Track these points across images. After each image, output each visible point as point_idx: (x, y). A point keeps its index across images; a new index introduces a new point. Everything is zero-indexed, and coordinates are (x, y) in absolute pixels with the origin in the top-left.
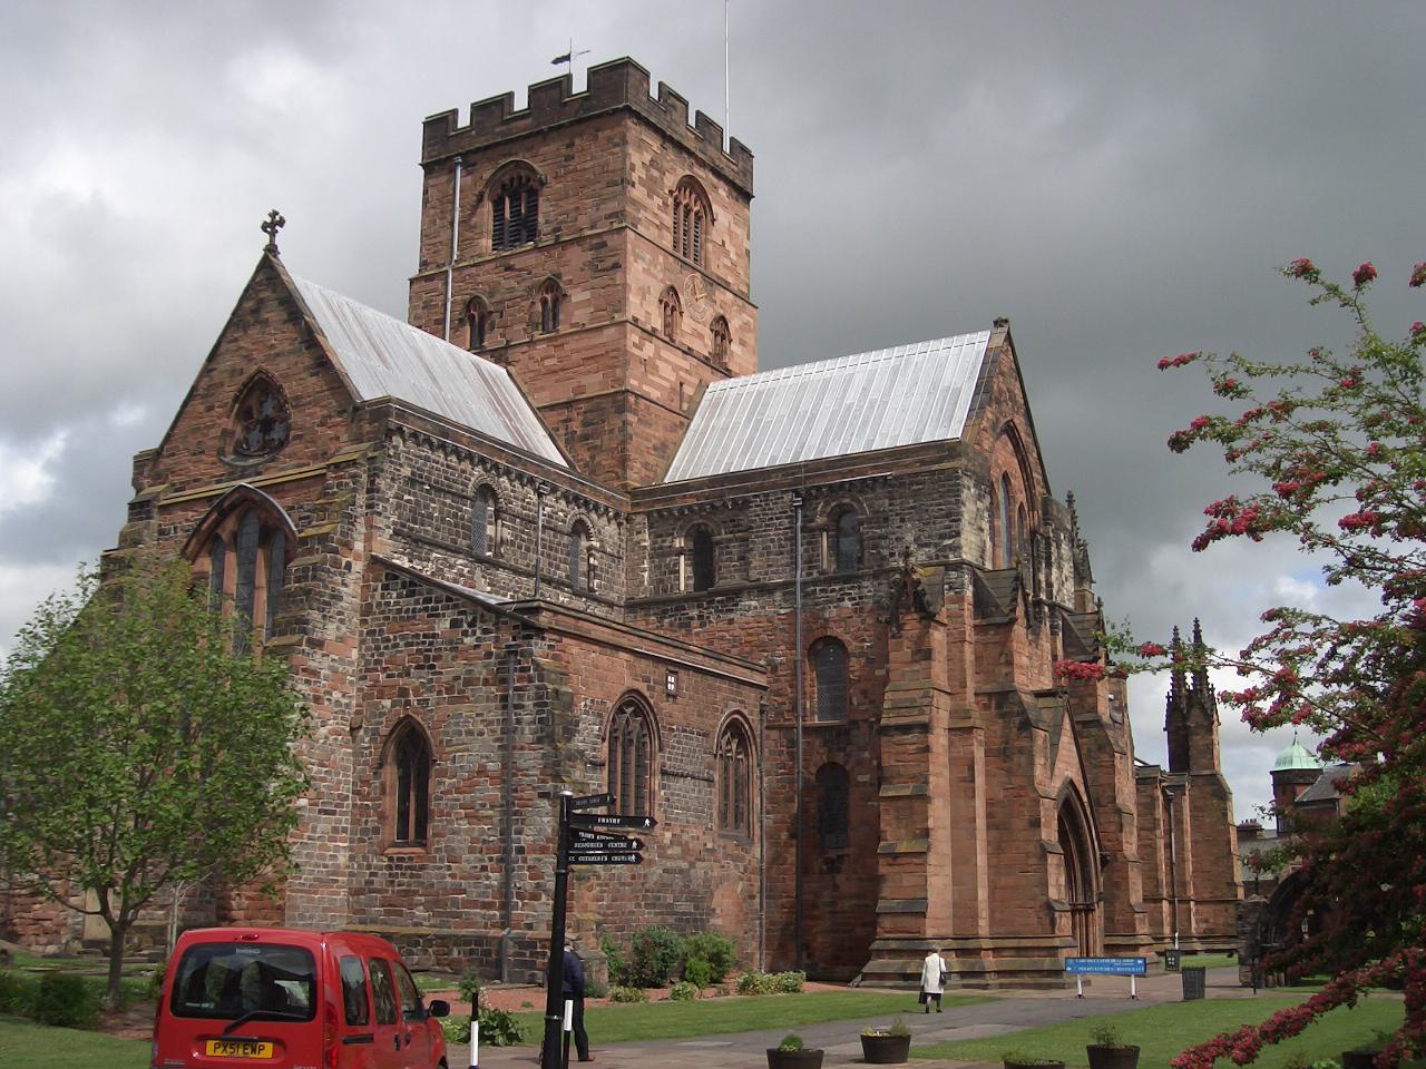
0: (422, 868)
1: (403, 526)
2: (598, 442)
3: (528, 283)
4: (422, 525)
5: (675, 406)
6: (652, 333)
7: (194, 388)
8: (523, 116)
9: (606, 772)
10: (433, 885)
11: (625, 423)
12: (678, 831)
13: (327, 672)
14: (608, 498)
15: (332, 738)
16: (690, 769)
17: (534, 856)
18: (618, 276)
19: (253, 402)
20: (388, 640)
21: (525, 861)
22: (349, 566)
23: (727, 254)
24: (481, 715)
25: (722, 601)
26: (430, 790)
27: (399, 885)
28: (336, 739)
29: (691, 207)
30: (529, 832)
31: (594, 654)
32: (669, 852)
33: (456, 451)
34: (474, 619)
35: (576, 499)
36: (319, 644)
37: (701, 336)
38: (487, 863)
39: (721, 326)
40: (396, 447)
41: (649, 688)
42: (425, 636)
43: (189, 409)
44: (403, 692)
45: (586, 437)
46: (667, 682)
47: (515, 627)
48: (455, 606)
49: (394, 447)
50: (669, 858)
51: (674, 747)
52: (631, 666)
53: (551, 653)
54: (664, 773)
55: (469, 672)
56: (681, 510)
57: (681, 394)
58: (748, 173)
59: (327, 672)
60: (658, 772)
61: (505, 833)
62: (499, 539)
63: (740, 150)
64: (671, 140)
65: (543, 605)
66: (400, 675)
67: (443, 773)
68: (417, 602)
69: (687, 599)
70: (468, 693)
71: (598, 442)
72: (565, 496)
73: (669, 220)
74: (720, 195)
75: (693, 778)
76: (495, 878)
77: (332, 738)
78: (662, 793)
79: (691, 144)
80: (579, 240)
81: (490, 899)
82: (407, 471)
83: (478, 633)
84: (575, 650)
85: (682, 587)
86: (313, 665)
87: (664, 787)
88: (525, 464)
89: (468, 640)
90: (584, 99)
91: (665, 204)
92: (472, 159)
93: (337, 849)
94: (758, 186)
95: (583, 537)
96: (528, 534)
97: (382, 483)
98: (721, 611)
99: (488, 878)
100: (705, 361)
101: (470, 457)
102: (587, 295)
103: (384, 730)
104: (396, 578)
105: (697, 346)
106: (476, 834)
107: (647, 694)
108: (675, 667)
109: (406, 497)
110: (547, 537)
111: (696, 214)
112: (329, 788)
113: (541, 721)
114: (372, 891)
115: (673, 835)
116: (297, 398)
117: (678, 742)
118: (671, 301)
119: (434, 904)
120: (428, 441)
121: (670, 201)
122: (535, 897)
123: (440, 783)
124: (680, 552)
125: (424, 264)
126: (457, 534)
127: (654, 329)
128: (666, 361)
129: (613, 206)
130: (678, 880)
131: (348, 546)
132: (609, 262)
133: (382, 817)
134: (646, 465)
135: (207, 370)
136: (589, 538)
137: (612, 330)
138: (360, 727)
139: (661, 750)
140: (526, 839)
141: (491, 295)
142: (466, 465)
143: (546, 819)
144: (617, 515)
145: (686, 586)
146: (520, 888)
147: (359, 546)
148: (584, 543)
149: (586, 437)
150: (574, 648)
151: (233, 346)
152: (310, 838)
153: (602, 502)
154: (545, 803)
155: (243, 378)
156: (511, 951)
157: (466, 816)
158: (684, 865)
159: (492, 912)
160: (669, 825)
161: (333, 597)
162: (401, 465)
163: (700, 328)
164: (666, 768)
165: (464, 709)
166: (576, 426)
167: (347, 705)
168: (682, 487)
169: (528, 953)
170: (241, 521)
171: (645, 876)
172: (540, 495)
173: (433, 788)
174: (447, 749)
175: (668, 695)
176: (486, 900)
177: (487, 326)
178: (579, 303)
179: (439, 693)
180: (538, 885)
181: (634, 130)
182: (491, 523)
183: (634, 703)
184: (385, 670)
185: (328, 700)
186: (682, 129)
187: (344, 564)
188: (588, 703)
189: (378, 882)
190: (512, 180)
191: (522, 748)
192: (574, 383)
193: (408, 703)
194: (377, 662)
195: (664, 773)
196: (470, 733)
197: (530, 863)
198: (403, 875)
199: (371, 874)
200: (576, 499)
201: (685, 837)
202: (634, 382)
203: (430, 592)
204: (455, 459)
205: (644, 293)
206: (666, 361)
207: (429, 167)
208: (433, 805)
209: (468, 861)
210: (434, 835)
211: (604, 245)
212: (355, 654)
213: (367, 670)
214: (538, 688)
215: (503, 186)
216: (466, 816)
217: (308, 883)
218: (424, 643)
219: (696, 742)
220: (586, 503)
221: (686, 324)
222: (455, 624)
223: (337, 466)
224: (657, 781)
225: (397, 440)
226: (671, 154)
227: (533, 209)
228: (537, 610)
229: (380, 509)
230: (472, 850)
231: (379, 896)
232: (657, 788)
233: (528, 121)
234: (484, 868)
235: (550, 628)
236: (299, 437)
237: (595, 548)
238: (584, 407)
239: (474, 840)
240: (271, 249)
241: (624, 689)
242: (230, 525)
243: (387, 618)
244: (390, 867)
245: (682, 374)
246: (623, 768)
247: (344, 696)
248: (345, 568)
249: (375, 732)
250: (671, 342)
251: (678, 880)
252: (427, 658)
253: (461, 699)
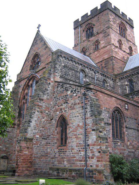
0: (66, 152)
1: (63, 76)
2: (108, 67)
3: (93, 42)
4: (67, 76)
5: (123, 60)
6: (117, 47)
7: (26, 59)
8: (90, 15)
9: (111, 126)
10: (68, 156)
11: (113, 62)
12: (131, 142)
13: (44, 106)
14: (110, 76)
15: (46, 121)
16: (133, 127)
17: (92, 147)
18: (109, 37)
19: (36, 59)
20: (58, 98)
21: (89, 148)
22: (50, 84)
23: (130, 36)
24: (78, 112)
25: (137, 93)
26: (67, 132)
27: (61, 156)
28: (47, 122)
29: (123, 32)
30: (90, 140)
31: (106, 97)
32: (129, 147)
33: (75, 61)
34: (76, 89)
35: (103, 75)
36: (42, 100)
37: (126, 49)
38: (80, 149)
39: (130, 48)
40: (60, 59)
41: (121, 107)
42: (65, 96)
43: (25, 63)
44: (61, 109)
45: (105, 67)
46: (125, 106)
47: (85, 89)
48: (72, 87)
49: (60, 59)
50: (129, 149)
51: (128, 122)
52: (116, 101)
53: (94, 95)
54: (126, 127)
55: (75, 102)
56: (126, 77)
57: (124, 59)
58: (132, 24)
59: (44, 106)
60: (125, 127)
61: (85, 141)
62: (86, 81)
63: (130, 19)
64: (117, 15)
65: (91, 83)
66: (61, 106)
67: (70, 127)
68: (64, 89)
69: (129, 94)
70: (75, 107)
71: (108, 67)
72: (101, 74)
73: (118, 29)
74: (128, 27)
75: (134, 129)
76: (83, 153)
77: (46, 121)
78: (126, 133)
79: (121, 17)
80: (101, 32)
81: (81, 159)
82: (63, 65)
83: (77, 92)
84: (101, 95)
85: (127, 92)
86: (40, 104)
87: (127, 131)
88: (91, 67)
89: (75, 95)
90: (100, 9)
91: (117, 26)
92: (82, 25)
93: (48, 148)
94: (135, 26)
95: (106, 83)
96: (93, 81)
97: (57, 66)
98: (137, 96)
99: (81, 153)
100: (128, 54)
101: (78, 63)
102: (103, 42)
103: (57, 119)
104: (59, 84)
105: (126, 51)
106: (78, 142)
107: (121, 108)
108: (127, 103)
109: (63, 70)
110: (97, 82)
111: (123, 29)
112: (45, 133)
113: (92, 111)
114: (55, 158)
115: (130, 143)
116: (42, 55)
117: (130, 121)
118: (120, 42)
119: (69, 161)
120: (68, 59)
121: (118, 25)
122: (92, 158)
123: (69, 130)
124: (127, 85)
125: (75, 45)
126: (76, 79)
127: (117, 46)
128: (120, 52)
129: (107, 25)
130: (132, 154)
131: (50, 79)
132: (107, 35)
133: (58, 140)
134: (118, 71)
135: (28, 56)
136: (107, 83)
137: (109, 46)
138: (53, 119)
139: (125, 122)
140: (90, 142)
141: (86, 46)
142: (77, 65)
143: (94, 136)
144: (113, 79)
145: (128, 92)
146: (88, 156)
147: (52, 79)
148: (106, 85)
149: (105, 67)
150: (101, 95)
151: (32, 50)
152: (40, 145)
153: (109, 76)
154: (93, 132)
155: (34, 55)
156: (87, 173)
157: (75, 137)
158: (134, 151)
159: (82, 162)
160: (129, 140)
161: (46, 90)
162: (62, 63)
163: (127, 48)
164: (127, 126)
165: (74, 111)
166: (103, 65)
167: (50, 114)
168: (126, 72)
169: (91, 174)
170: (33, 81)
171: (124, 153)
172: (95, 73)
173: (68, 131)
174: (71, 121)
175: (126, 109)
176: (80, 159)
177: (86, 52)
178: (102, 43)
179: (69, 108)
180: (93, 155)
181: (110, 13)
182: (84, 78)
183: (117, 110)
184: (57, 105)
185: (45, 112)
186: (119, 14)
187: (48, 83)
188: (105, 108)
189: (57, 155)
190: (89, 27)
191: (88, 119)
192: (102, 58)
193: (62, 112)
194: (56, 104)
195: (126, 127)
196: (75, 117)
197: (91, 149)
198: (62, 153)
199: (55, 154)
200: (103, 75)
201: (133, 144)
202: (114, 55)
203: (66, 86)
204: (75, 64)
205: (115, 40)
206: (120, 52)
207: (75, 29)
208: (68, 136)
209: (76, 149)
210: (68, 143)
211: (106, 32)
212: (52, 103)
213: (54, 106)
214: (90, 103)
215: (87, 29)
216: (75, 137)
217: (39, 156)
218: (65, 97)
219: (134, 121)
220: (106, 76)
221: (124, 47)
222: (72, 91)
223: (48, 64)
224: (125, 129)
225: (60, 58)
226: (117, 18)
227: (93, 31)
228: (90, 84)
229: (57, 71)
230: (77, 146)
231: (57, 159)
232: (125, 131)
233: (91, 16)
234: (80, 151)
235: (93, 89)
236: (42, 62)
237: (108, 86)
238: (104, 61)
239: (77, 144)
240: (39, 31)
241: (114, 106)
242: (31, 82)
243: (58, 94)
244: (59, 152)
245: (124, 55)
246: (116, 126)
247: (49, 112)
248: (49, 84)
249: (56, 120)
250: (121, 49)
251: (132, 154)
252: (66, 101)
253: (74, 109)
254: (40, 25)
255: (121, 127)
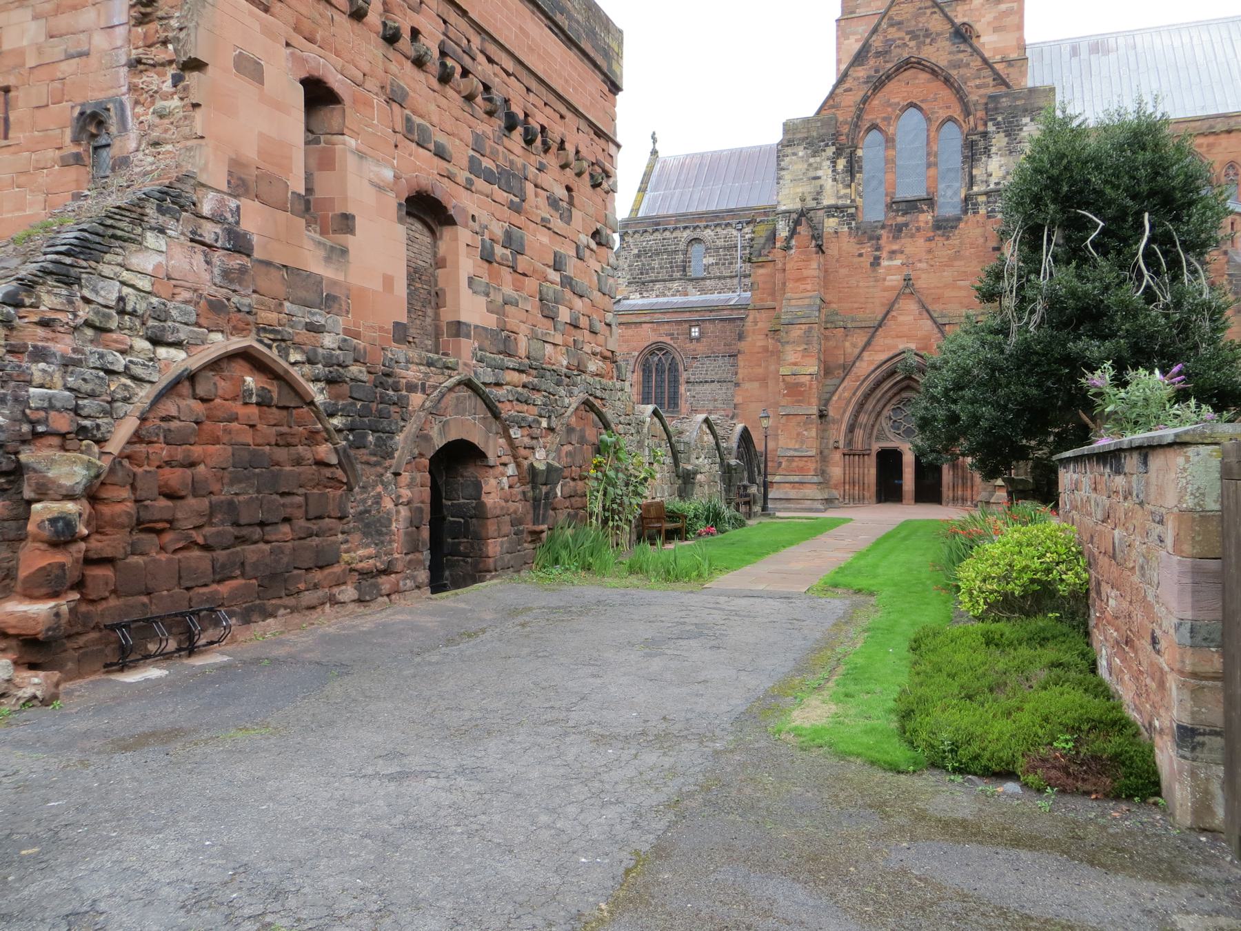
52: (654, 330)
82: (636, 251)
87: (689, 390)
107: (671, 342)
164: (692, 380)
254: (654, 133)
255: (675, 382)
